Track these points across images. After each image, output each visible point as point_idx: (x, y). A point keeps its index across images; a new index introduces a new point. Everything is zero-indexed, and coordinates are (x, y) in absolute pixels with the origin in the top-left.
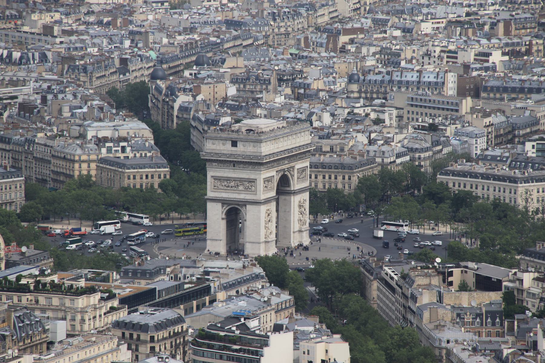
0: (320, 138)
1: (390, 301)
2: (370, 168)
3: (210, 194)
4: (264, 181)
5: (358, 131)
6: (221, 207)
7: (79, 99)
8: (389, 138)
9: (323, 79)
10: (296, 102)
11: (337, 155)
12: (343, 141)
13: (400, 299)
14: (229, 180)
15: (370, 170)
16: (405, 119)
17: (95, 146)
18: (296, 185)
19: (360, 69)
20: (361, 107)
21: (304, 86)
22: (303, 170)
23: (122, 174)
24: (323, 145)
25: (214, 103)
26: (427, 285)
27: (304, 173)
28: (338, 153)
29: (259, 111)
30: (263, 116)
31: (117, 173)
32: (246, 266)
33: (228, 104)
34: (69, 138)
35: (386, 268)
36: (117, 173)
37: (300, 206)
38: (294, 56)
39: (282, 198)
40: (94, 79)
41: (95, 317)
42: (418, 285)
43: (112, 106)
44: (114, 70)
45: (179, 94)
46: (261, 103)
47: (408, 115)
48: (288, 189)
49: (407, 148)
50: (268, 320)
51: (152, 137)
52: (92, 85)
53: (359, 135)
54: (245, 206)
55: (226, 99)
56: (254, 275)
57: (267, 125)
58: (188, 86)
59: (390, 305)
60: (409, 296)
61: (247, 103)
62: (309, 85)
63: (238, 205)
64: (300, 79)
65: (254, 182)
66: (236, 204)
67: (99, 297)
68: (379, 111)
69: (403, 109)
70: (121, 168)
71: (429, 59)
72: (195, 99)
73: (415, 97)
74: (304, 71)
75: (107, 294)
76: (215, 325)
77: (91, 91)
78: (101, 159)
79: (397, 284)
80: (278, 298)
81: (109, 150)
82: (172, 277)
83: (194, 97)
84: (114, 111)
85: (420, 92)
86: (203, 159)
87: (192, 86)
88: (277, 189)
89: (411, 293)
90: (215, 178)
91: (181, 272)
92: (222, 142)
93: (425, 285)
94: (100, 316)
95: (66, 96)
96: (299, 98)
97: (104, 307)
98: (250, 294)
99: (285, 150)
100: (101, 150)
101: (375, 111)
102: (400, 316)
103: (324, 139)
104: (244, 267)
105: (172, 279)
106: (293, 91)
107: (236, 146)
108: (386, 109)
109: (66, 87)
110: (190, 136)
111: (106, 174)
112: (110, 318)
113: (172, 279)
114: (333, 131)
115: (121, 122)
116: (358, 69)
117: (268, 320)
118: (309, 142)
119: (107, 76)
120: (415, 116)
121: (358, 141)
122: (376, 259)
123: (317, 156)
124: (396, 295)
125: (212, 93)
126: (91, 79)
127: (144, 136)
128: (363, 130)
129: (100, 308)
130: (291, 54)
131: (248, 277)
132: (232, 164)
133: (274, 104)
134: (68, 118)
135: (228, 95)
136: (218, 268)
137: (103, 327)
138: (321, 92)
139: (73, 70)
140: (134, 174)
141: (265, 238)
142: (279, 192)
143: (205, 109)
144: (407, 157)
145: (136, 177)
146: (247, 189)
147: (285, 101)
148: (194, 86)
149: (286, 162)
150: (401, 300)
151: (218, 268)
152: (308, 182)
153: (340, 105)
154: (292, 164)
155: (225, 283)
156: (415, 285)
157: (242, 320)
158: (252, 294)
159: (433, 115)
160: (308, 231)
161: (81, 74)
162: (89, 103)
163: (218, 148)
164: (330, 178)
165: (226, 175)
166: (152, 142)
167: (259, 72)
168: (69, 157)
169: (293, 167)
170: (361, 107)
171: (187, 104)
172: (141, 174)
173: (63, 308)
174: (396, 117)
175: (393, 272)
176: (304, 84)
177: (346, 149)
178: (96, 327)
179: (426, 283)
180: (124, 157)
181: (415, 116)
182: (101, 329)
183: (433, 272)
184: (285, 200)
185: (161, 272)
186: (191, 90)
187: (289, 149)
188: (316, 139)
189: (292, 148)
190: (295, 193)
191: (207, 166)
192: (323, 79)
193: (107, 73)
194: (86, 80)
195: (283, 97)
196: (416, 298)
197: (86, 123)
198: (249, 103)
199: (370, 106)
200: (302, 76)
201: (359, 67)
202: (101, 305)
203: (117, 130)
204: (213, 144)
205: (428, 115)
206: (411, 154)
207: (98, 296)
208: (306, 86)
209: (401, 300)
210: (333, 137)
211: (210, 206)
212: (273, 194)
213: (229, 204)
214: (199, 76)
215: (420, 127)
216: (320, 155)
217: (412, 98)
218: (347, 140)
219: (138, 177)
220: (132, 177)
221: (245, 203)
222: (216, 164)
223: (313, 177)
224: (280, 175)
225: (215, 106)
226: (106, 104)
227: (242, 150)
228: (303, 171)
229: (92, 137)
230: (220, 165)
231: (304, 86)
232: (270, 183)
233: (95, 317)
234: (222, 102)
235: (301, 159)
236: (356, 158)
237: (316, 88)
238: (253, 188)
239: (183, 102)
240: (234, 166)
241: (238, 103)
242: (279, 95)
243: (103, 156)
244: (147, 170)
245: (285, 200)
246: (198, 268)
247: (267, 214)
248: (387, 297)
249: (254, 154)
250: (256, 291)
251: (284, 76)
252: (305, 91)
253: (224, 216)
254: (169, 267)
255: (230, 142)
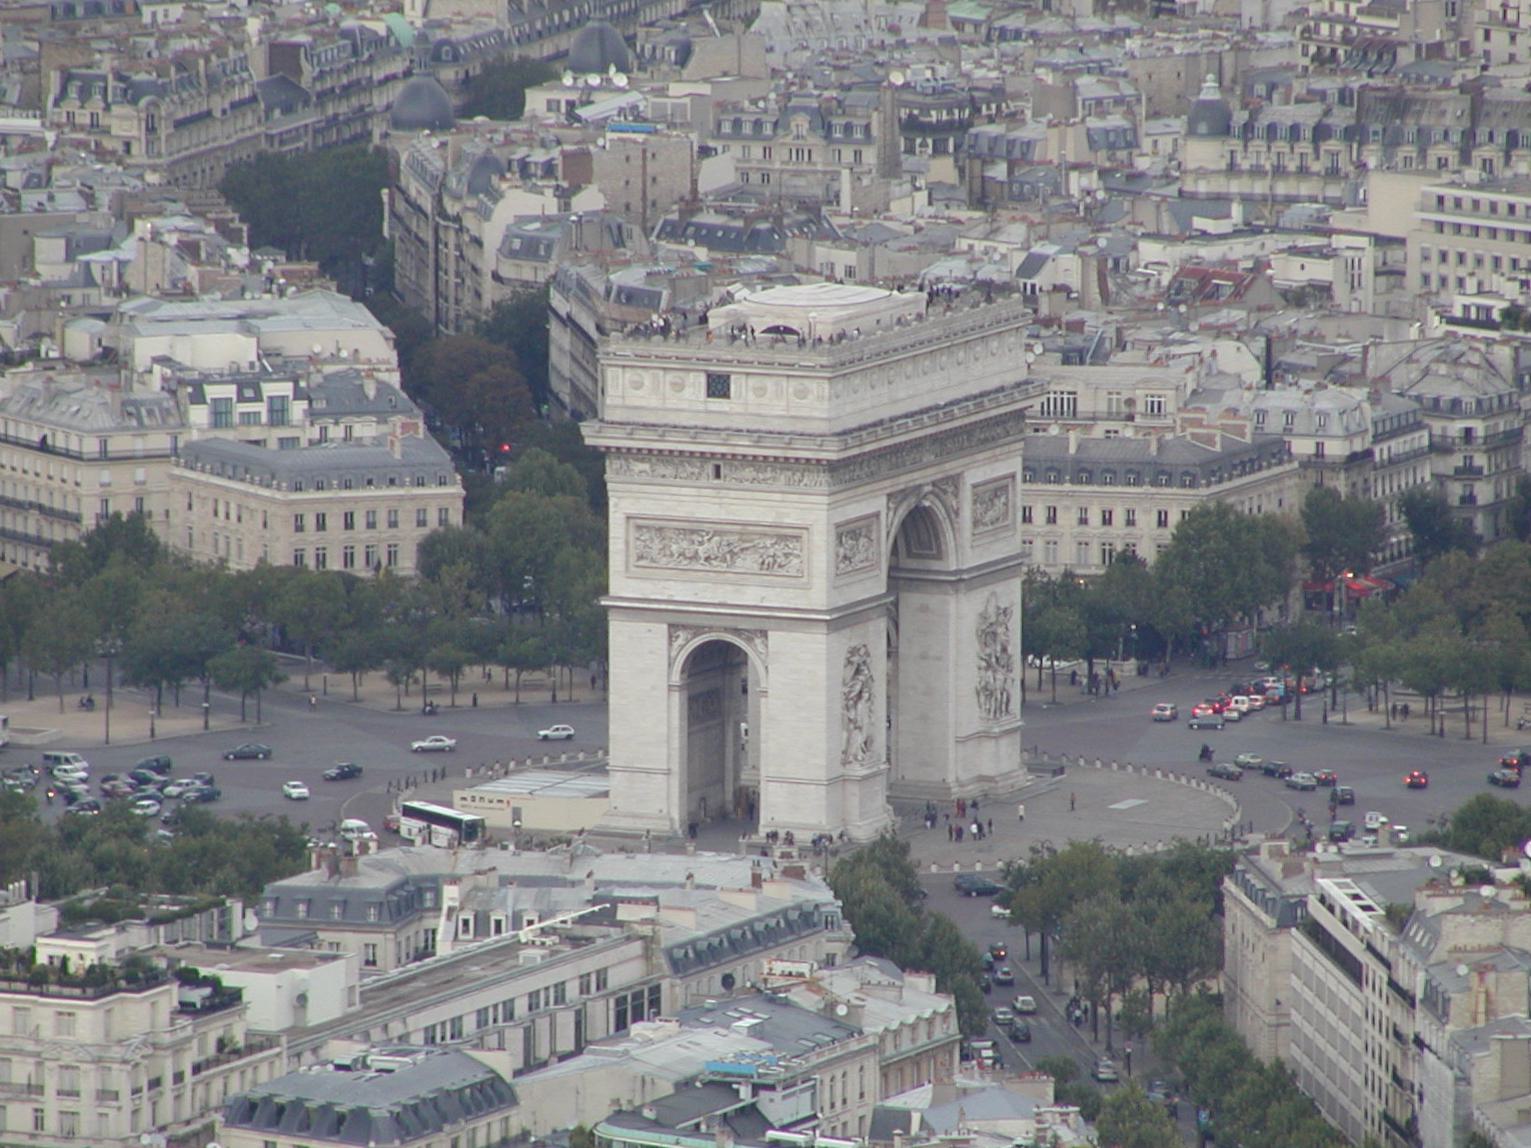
0: (1066, 361)
1: (1344, 1013)
2: (1269, 481)
3: (622, 584)
4: (839, 537)
5: (1221, 331)
6: (665, 641)
7: (105, 210)
8: (1346, 359)
9: (1083, 120)
10: (978, 214)
11: (1137, 429)
12: (1157, 372)
13: (1381, 1005)
14: (693, 532)
15: (1271, 488)
16: (1413, 281)
17: (165, 395)
18: (964, 549)
19: (1234, 81)
20: (1237, 233)
21: (1009, 152)
22: (998, 489)
23: (272, 509)
24: (1080, 390)
25: (645, 220)
26: (1489, 949)
27: (1000, 502)
28: (1138, 420)
29: (823, 252)
30: (840, 273)
31: (253, 504)
32: (765, 875)
33: (699, 226)
34: (60, 366)
35: (1327, 884)
36: (253, 504)
37: (988, 634)
38: (969, 29)
39: (911, 600)
40: (164, 130)
41: (155, 1083)
42: (1457, 949)
43: (233, 237)
44: (237, 94)
45: (504, 186)
46: (836, 221)
47: (1427, 268)
48: (936, 565)
49: (1419, 398)
50: (853, 1095)
51: (392, 356)
52: (159, 155)
53: (1227, 348)
54: (764, 634)
55: (692, 203)
56: (794, 916)
57: (851, 311)
58: (539, 156)
59: (1344, 1030)
60: (1419, 995)
61: (778, 219)
62: (1029, 144)
63: (737, 631)
64: (991, 120)
65: (797, 538)
66: (726, 630)
67: (175, 1003)
68: (1306, 252)
69: (1402, 242)
70: (268, 486)
71: (1513, 38)
72: (567, 206)
73: (1450, 193)
74: (1009, 89)
75: (207, 991)
76: (636, 1113)
77: (152, 178)
78: (190, 446)
79: (1370, 948)
80: (894, 1007)
81: (220, 415)
82: (466, 923)
83: (564, 196)
84: (240, 256)
85: (1473, 174)
86: (595, 448)
87: (555, 153)
88: (893, 569)
89: (1428, 982)
90: (638, 523)
91: (503, 903)
92: (670, 377)
93: (1480, 950)
94: (178, 1077)
95: (51, 198)
96: (981, 199)
97: (195, 1043)
98: (775, 991)
99: (922, 412)
100: (186, 412)
101: (1293, 251)
102: (1381, 1073)
103: (1082, 362)
104: (757, 881)
105: (466, 930)
106: (961, 171)
107: (726, 394)
108: (1339, 241)
109: (50, 164)
110: (546, 355)
111: (210, 508)
112: (217, 1086)
113: (466, 930)
114: (1119, 331)
115: (266, 301)
116: (1227, 82)
117: (853, 1095)
118: (1022, 375)
119: (217, 114)
120: (1452, 270)
121: (1220, 373)
122: (1286, 845)
123: (1054, 430)
124: (1368, 990)
125: (637, 183)
126: (151, 129)
127: (363, 356)
128: (1241, 328)
129: (177, 1048)
130: (958, 24)
131: (772, 923)
132: (710, 468)
133: (887, 224)
134: (60, 285)
135: (702, 188)
136: (652, 885)
137: (188, 1123)
138: (1074, 175)
139: (85, 95)
140: (321, 509)
141: (845, 763)
142: (898, 579)
143: (608, 243)
144: (1417, 435)
145: (329, 522)
146: (768, 566)
147: (932, 210)
148: (565, 155)
149: (929, 458)
150: (1387, 1012)
151: (652, 885)
152: (1019, 538)
153: (1152, 229)
154: (951, 467)
155: (681, 946)
156: (1441, 952)
157: (745, 1092)
158: (787, 989)
159: (1523, 264)
160: (1017, 737)
161: (116, 109)
162: (143, 227)
163: (654, 402)
164: (1107, 520)
165: (682, 511)
166: (394, 379)
167: (827, 94)
168: (60, 442)
169: (955, 480)
170: (1237, 233)
171: (537, 225)
172: (348, 508)
173: (30, 1047)
174: (1377, 274)
175: (1356, 897)
176: (1012, 143)
177: (1170, 407)
178: (160, 1122)
179: (1484, 943)
180: (281, 440)
181: (1452, 270)
182: (183, 1131)
183: (1514, 898)
184: (924, 609)
185: (421, 900)
186: (549, 169)
187: (937, 407)
188: (1052, 366)
189: (952, 403)
190: (961, 582)
191: (608, 476)
192: (1083, 120)
193: (218, 104)
194: (135, 133)
195: (922, 197)
196: (1447, 1001)
197: (128, 306)
198: (786, 221)
199: (1275, 229)
200: (998, 108)
201: (1228, 75)
202: (181, 1035)
203: (248, 331)
204: (638, 386)
205: (1506, 265)
206: (1437, 426)
207: (170, 995)
208: (1017, 153)
209: (1387, 1012)
210: (1120, 357)
211: (621, 635)
212: (875, 585)
213: (697, 630)
214: (583, 112)
215: (1473, 316)
216: (1067, 428)
217: (1441, 200)
218: (1176, 369)
219: (335, 522)
220: (310, 522)
221: (761, 625)
222: (646, 466)
223: (1039, 515)
224: (902, 512)
225: (647, 232)
226: (211, 230)
227: (752, 409)
228: (996, 494)
229: (157, 360)
230: (661, 469)
231: (1009, 152)
232: (863, 541)
233: (155, 1083)
234: (675, 217)
235: (987, 443)
236: (1210, 440)
237: (1053, 155)
238: (795, 561)
239: (522, 220)
240: (718, 475)
241: (739, 223)
242: (907, 187)
243: (195, 436)
244: (371, 492)
245: (924, 609)
246: (573, 884)
247: (851, 671)
248: (1333, 1002)
249: (799, 427)
250: (801, 975)
251: (925, 109)
252: (1010, 172)
253: (676, 678)
254: (455, 880)
255: (703, 379)
